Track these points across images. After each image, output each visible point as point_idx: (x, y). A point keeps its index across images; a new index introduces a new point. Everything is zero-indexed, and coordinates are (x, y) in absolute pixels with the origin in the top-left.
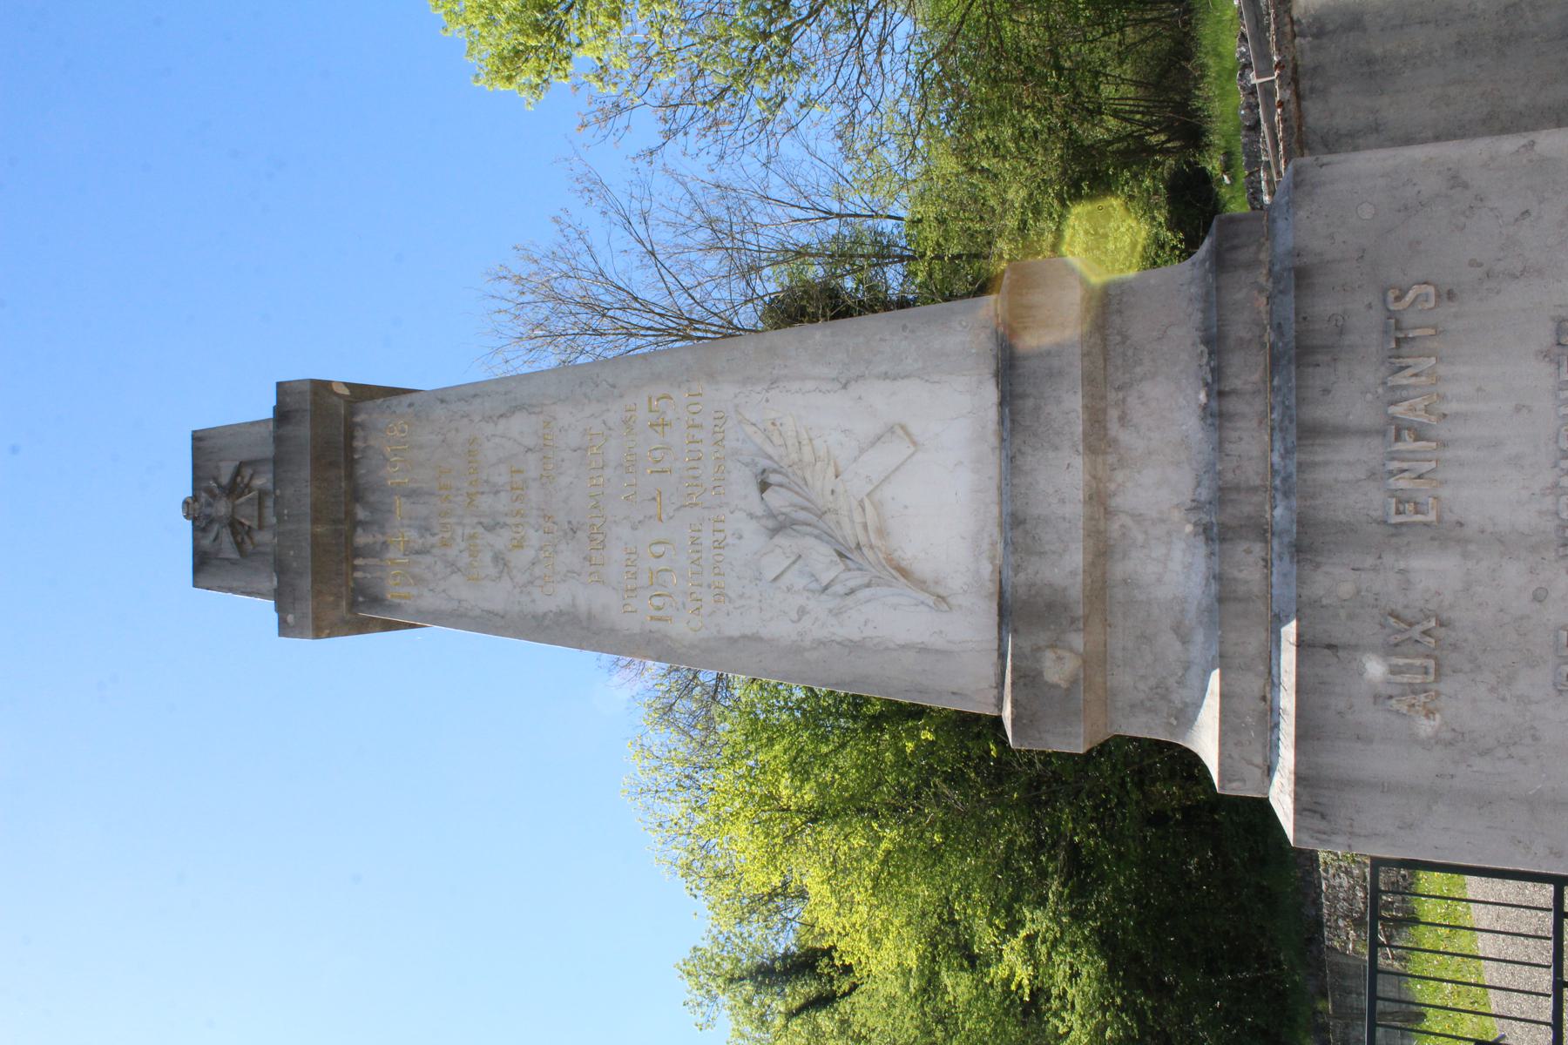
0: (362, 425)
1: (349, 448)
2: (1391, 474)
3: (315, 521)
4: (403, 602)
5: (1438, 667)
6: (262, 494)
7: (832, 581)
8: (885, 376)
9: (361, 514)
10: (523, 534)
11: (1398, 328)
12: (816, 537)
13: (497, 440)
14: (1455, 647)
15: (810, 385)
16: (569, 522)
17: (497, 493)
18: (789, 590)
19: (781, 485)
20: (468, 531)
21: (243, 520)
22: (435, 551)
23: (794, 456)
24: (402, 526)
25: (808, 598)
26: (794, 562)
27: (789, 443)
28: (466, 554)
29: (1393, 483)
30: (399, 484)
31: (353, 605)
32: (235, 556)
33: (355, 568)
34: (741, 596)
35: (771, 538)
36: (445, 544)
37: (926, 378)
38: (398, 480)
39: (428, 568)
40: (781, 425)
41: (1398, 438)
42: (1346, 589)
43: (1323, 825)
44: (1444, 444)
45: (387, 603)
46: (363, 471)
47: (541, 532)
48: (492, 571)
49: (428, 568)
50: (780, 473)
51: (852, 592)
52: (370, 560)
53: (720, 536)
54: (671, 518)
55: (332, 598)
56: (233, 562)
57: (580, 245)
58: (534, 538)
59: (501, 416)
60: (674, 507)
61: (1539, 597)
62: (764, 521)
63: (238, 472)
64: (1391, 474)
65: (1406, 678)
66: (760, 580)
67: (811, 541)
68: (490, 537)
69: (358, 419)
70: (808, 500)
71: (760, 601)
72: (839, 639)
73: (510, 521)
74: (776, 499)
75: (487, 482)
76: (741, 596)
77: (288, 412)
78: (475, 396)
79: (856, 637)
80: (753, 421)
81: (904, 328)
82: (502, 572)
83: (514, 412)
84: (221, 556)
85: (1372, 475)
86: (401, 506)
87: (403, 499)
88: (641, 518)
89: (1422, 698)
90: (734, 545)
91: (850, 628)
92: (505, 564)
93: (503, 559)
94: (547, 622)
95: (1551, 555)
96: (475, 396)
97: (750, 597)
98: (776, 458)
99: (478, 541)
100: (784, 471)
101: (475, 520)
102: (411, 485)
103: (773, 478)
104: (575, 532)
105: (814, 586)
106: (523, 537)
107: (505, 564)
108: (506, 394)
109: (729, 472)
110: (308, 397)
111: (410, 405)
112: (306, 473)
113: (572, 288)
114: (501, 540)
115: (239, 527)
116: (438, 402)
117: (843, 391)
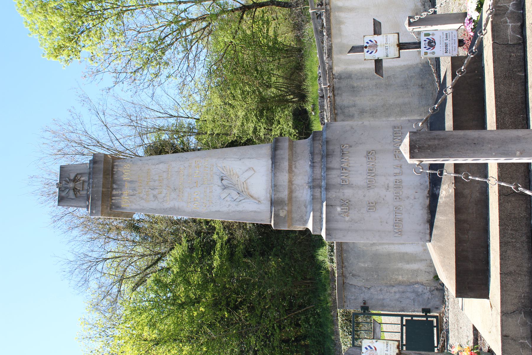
0: (117, 165)
1: (113, 171)
2: (341, 176)
3: (103, 188)
5: (349, 208)
6: (84, 182)
8: (249, 158)
9: (115, 186)
11: (343, 151)
13: (156, 169)
14: (351, 205)
15: (233, 159)
22: (136, 195)
23: (229, 174)
29: (342, 177)
31: (111, 208)
32: (74, 197)
33: (112, 199)
34: (216, 203)
36: (139, 193)
39: (135, 199)
41: (342, 170)
42: (334, 196)
43: (330, 237)
44: (350, 171)
48: (153, 199)
49: (135, 199)
51: (241, 201)
56: (72, 199)
57: (77, 121)
58: (164, 191)
61: (364, 196)
63: (76, 176)
64: (341, 176)
65: (344, 210)
68: (153, 191)
69: (115, 164)
73: (158, 188)
76: (216, 203)
79: (241, 210)
84: (69, 197)
85: (338, 176)
86: (127, 185)
89: (346, 214)
91: (240, 208)
95: (366, 189)
103: (224, 178)
105: (232, 200)
110: (103, 158)
111: (131, 161)
112: (102, 176)
113: (74, 136)
114: (155, 192)
115: (75, 190)
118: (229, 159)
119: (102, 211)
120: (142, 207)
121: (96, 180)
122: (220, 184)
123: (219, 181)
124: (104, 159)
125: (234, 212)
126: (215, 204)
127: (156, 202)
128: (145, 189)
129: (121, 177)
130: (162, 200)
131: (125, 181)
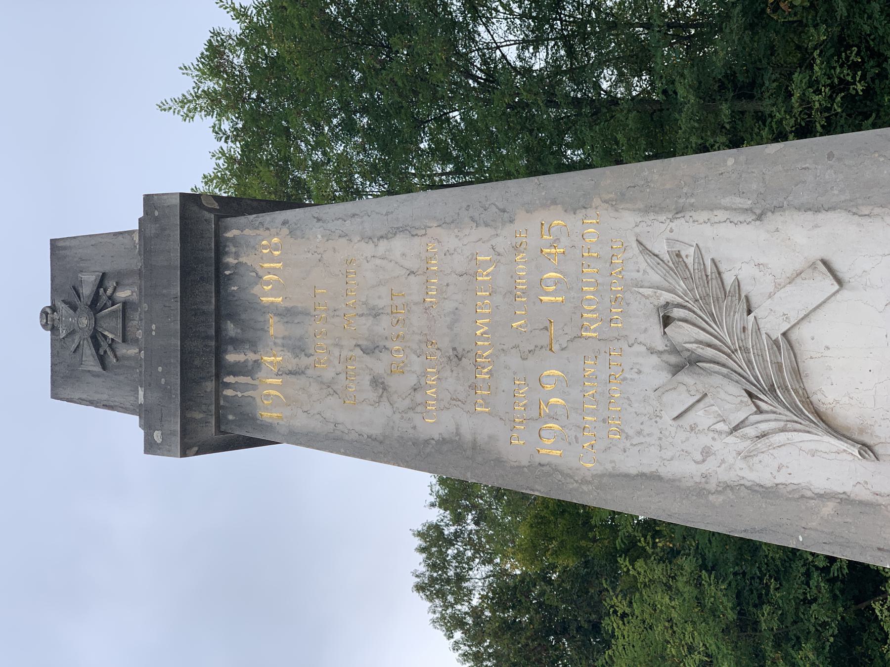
0: (233, 240)
1: (219, 265)
7: (742, 422)
12: (725, 376)
13: (378, 262)
15: (721, 215)
16: (454, 349)
17: (376, 316)
18: (692, 429)
19: (685, 321)
20: (345, 353)
21: (106, 333)
25: (713, 439)
26: (698, 401)
30: (272, 303)
32: (98, 369)
34: (639, 433)
35: (674, 375)
37: (854, 210)
45: (258, 422)
46: (235, 288)
47: (423, 358)
48: (372, 395)
51: (764, 435)
54: (563, 349)
59: (382, 237)
60: (568, 337)
62: (666, 357)
63: (101, 282)
67: (717, 380)
69: (229, 235)
70: (716, 337)
71: (660, 439)
72: (748, 484)
74: (682, 333)
76: (639, 433)
78: (354, 215)
81: (830, 156)
82: (381, 396)
83: (395, 234)
86: (274, 327)
87: (276, 319)
88: (532, 348)
90: (632, 380)
92: (384, 389)
93: (383, 383)
96: (354, 215)
101: (354, 343)
102: (284, 305)
103: (677, 313)
104: (460, 359)
105: (721, 426)
108: (387, 214)
109: (628, 304)
111: (285, 223)
114: (379, 365)
117: (758, 223)
118: (703, 216)
123: (656, 328)
126: (635, 441)
127: (385, 409)
129: (256, 290)
130: (407, 402)
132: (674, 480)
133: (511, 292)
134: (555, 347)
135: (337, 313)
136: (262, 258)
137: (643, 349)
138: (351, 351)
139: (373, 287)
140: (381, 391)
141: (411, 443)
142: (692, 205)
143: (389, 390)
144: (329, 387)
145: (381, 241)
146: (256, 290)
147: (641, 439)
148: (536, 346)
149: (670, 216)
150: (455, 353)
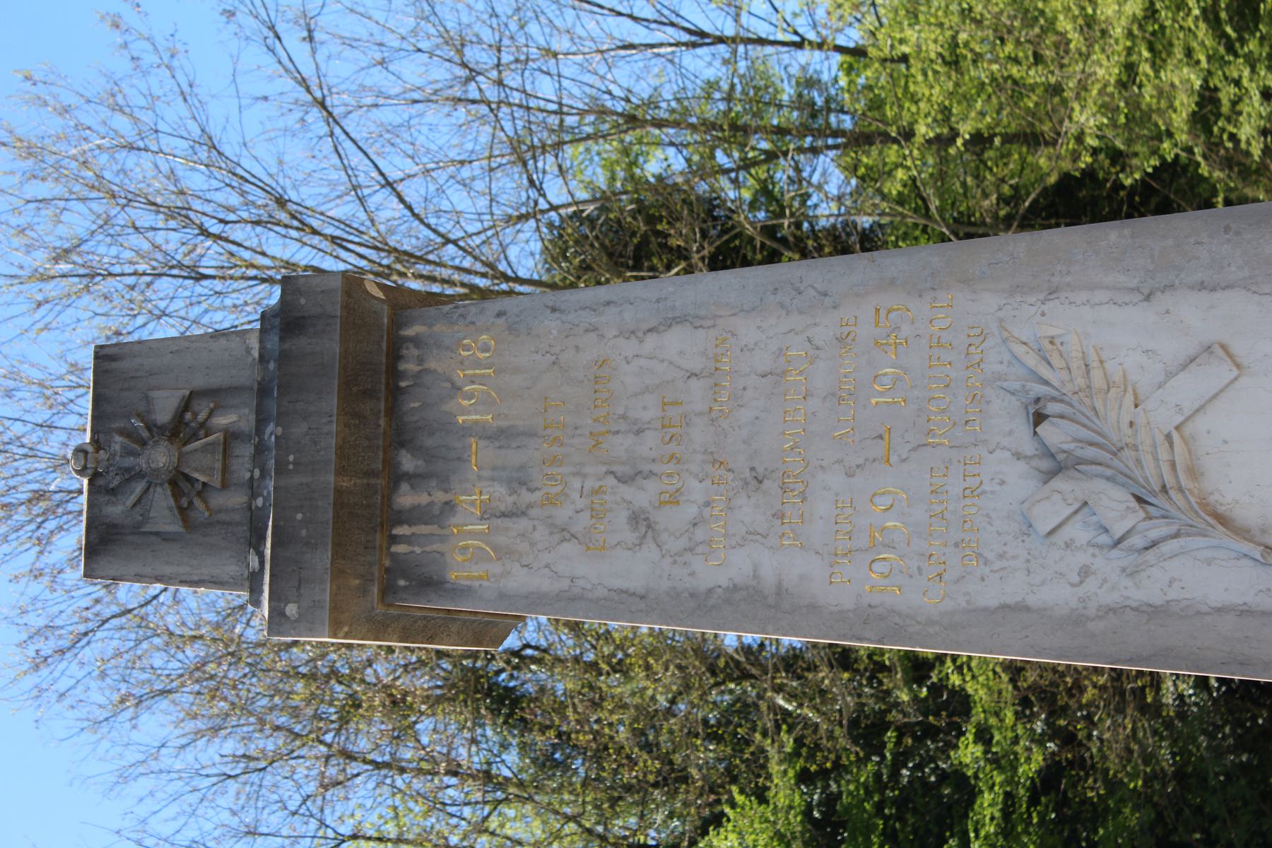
0: (417, 341)
1: (394, 373)
3: (340, 471)
4: (476, 584)
6: (231, 436)
7: (1128, 532)
8: (1202, 286)
9: (408, 462)
10: (678, 486)
12: (1108, 479)
13: (642, 362)
15: (1101, 296)
16: (753, 469)
18: (1067, 546)
19: (1062, 417)
20: (590, 484)
21: (196, 475)
22: (534, 512)
23: (1080, 381)
24: (480, 478)
25: (1093, 555)
26: (1076, 512)
27: (1074, 365)
28: (587, 514)
30: (476, 422)
31: (388, 591)
32: (175, 527)
33: (394, 540)
34: (1001, 556)
35: (1045, 483)
36: (550, 501)
37: (1254, 289)
38: (474, 417)
39: (522, 535)
40: (1062, 344)
45: (448, 586)
47: (708, 483)
48: (630, 537)
49: (522, 535)
50: (1062, 401)
51: (1154, 544)
52: (423, 527)
53: (971, 482)
54: (904, 461)
55: (357, 582)
56: (166, 538)
57: (160, 82)
58: (697, 490)
59: (650, 330)
60: (909, 446)
62: (1035, 462)
63: (186, 405)
66: (1029, 535)
67: (1100, 484)
68: (626, 491)
69: (410, 332)
70: (1099, 434)
71: (1028, 561)
72: (1134, 604)
73: (656, 468)
74: (1052, 433)
75: (624, 417)
76: (1001, 556)
77: (304, 317)
78: (608, 303)
79: (1158, 600)
80: (1024, 339)
81: (1227, 229)
82: (644, 536)
83: (670, 326)
84: (148, 528)
86: (479, 454)
87: (482, 443)
88: (861, 461)
90: (993, 492)
92: (649, 527)
93: (646, 519)
94: (712, 601)
96: (608, 303)
97: (1014, 557)
98: (1056, 383)
99: (606, 497)
100: (1067, 399)
101: (604, 469)
103: (1052, 408)
104: (760, 482)
105: (1104, 539)
106: (678, 490)
107: (649, 527)
108: (658, 301)
109: (988, 403)
110: (339, 298)
111: (500, 314)
112: (332, 403)
113: (141, 169)
114: (643, 496)
115: (184, 485)
116: (548, 311)
117: (1146, 303)
118: (1083, 296)
119: (335, 608)
120: (565, 584)
121: (299, 429)
122: (1029, 447)
123: (1023, 429)
124: (346, 307)
125: (1111, 610)
127: (650, 551)
128: (585, 476)
129: (447, 407)
130: (683, 542)
131: (467, 431)
132: (1045, 609)
133: (833, 395)
134: (893, 459)
135: (578, 432)
136: (462, 363)
137: (1008, 454)
138: (600, 480)
139: (636, 395)
140: (643, 530)
141: (686, 595)
142: (1068, 285)
143: (657, 527)
144: (564, 530)
145: (649, 335)
146: (449, 407)
147: (1004, 563)
148: (867, 460)
149: (1041, 297)
150: (754, 474)
